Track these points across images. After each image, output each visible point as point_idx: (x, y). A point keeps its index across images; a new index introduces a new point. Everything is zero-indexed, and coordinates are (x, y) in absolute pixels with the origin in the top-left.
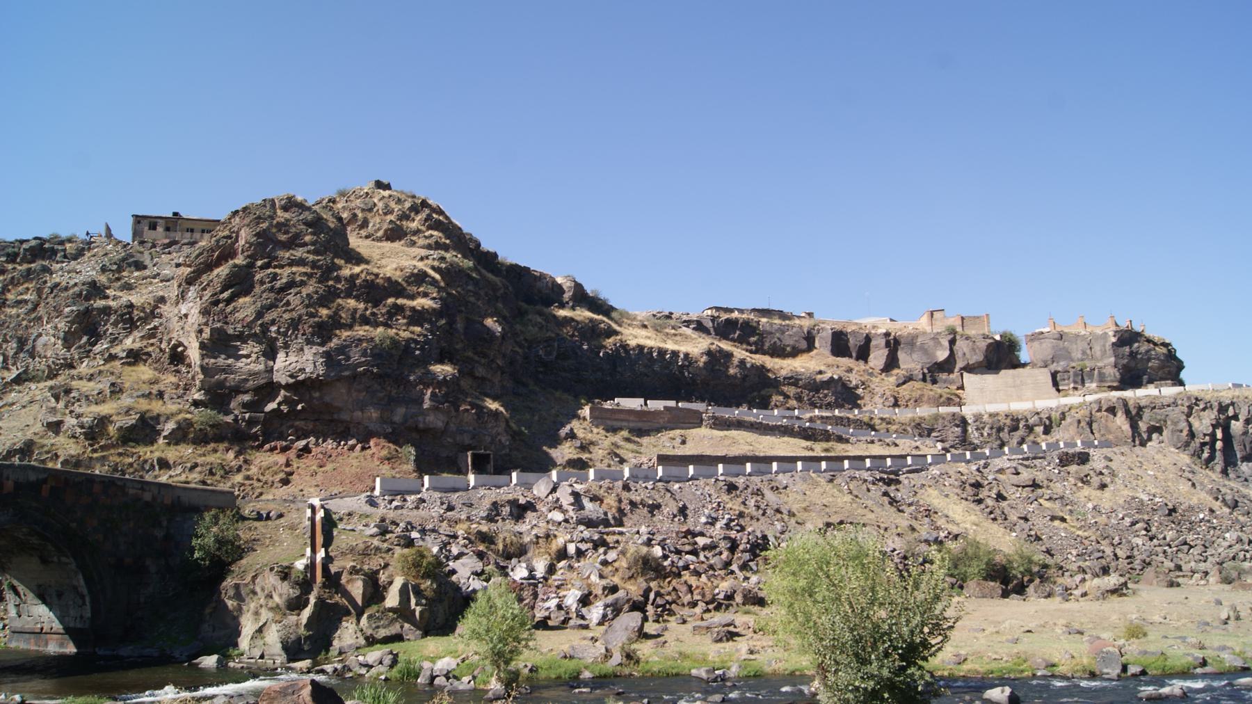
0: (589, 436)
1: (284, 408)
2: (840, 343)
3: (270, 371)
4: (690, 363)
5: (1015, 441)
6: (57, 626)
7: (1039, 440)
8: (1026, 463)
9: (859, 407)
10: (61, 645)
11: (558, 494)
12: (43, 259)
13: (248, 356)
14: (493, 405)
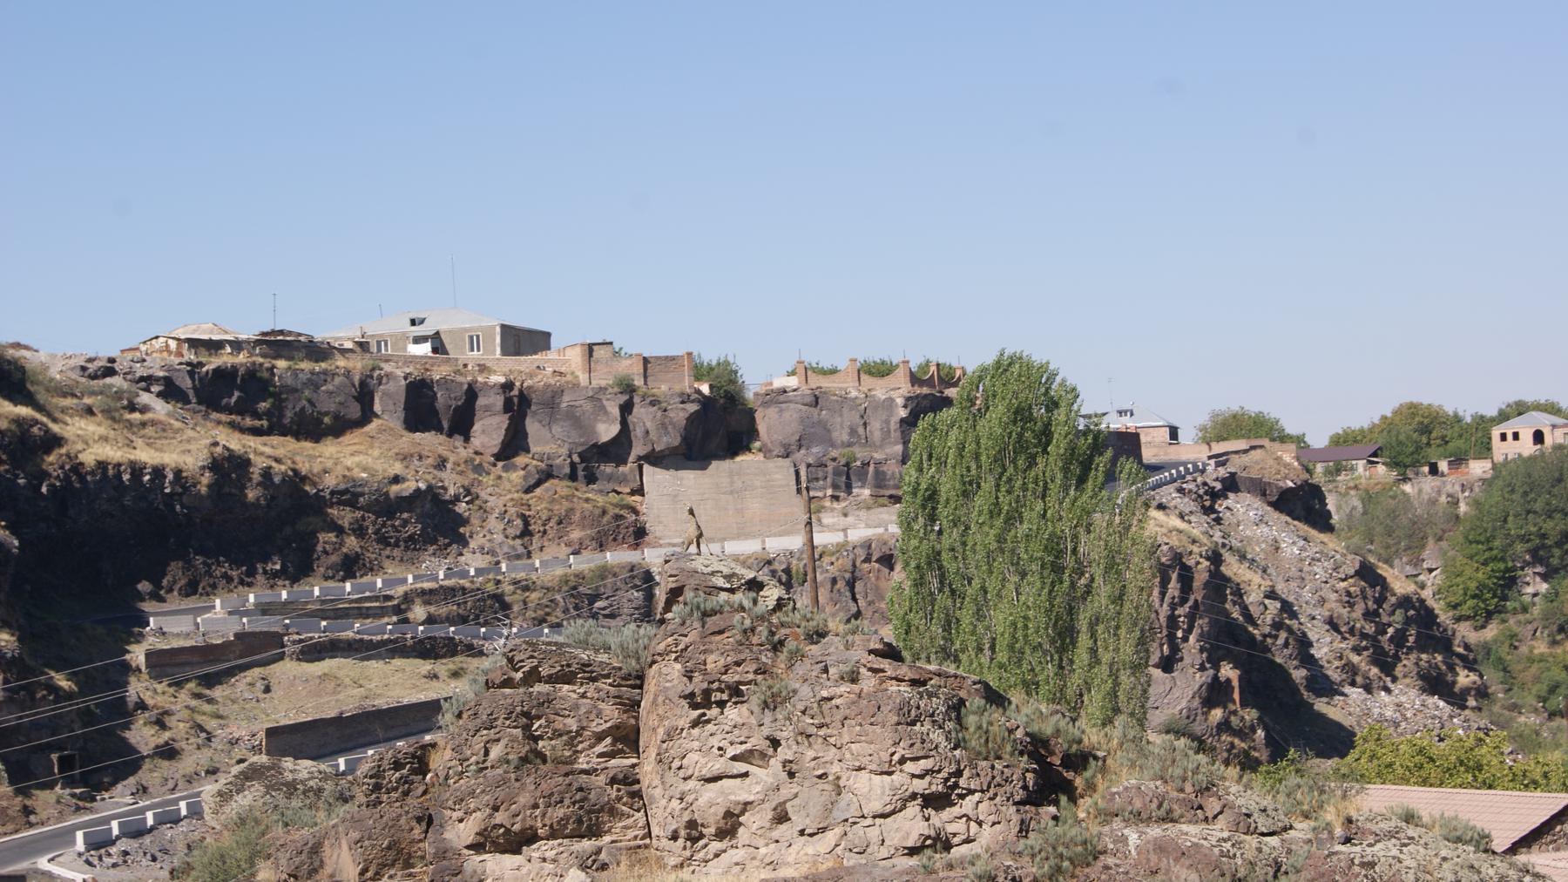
2: (425, 407)
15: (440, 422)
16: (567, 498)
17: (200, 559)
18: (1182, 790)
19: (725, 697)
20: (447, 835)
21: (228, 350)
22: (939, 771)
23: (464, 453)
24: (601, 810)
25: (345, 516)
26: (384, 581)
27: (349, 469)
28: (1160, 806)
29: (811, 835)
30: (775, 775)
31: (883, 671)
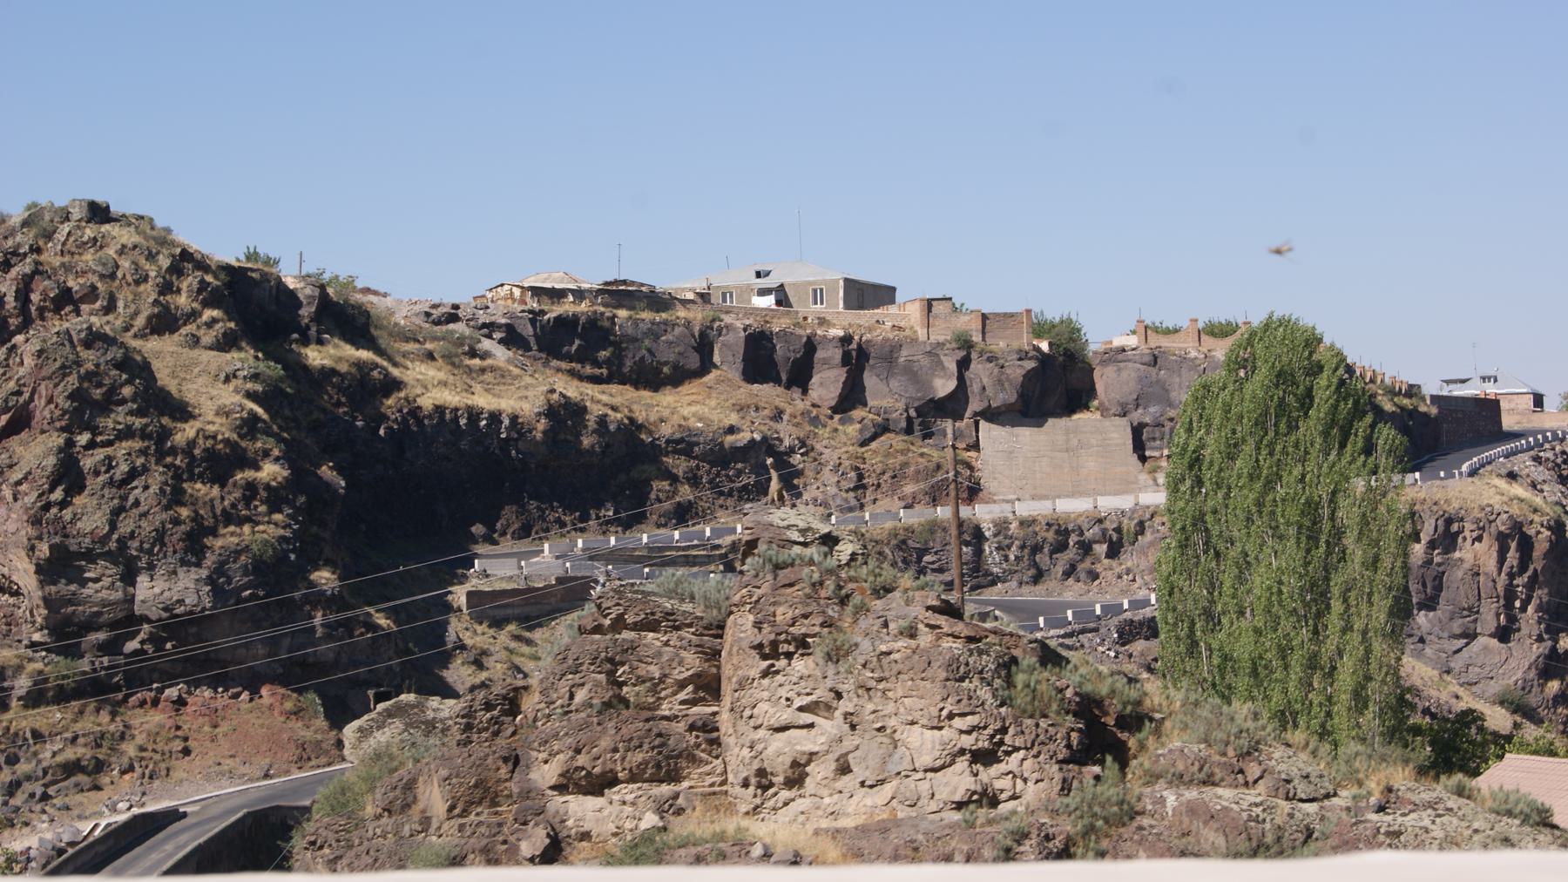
1: (148, 647)
2: (762, 358)
3: (131, 600)
5: (1059, 570)
7: (1098, 568)
8: (1068, 641)
15: (778, 373)
16: (902, 452)
17: (534, 504)
18: (1224, 754)
19: (792, 649)
20: (532, 776)
21: (571, 298)
22: (985, 728)
23: (800, 405)
24: (679, 756)
25: (680, 465)
26: (712, 530)
27: (685, 419)
28: (1201, 769)
29: (871, 787)
30: (839, 727)
31: (939, 627)
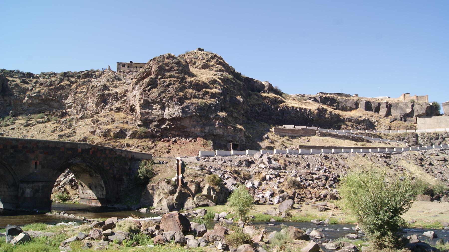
0: (274, 138)
1: (168, 127)
2: (368, 106)
3: (163, 114)
4: (311, 113)
5: (437, 144)
6: (95, 197)
9: (375, 130)
10: (96, 203)
11: (263, 158)
12: (89, 77)
13: (156, 109)
14: (240, 127)
